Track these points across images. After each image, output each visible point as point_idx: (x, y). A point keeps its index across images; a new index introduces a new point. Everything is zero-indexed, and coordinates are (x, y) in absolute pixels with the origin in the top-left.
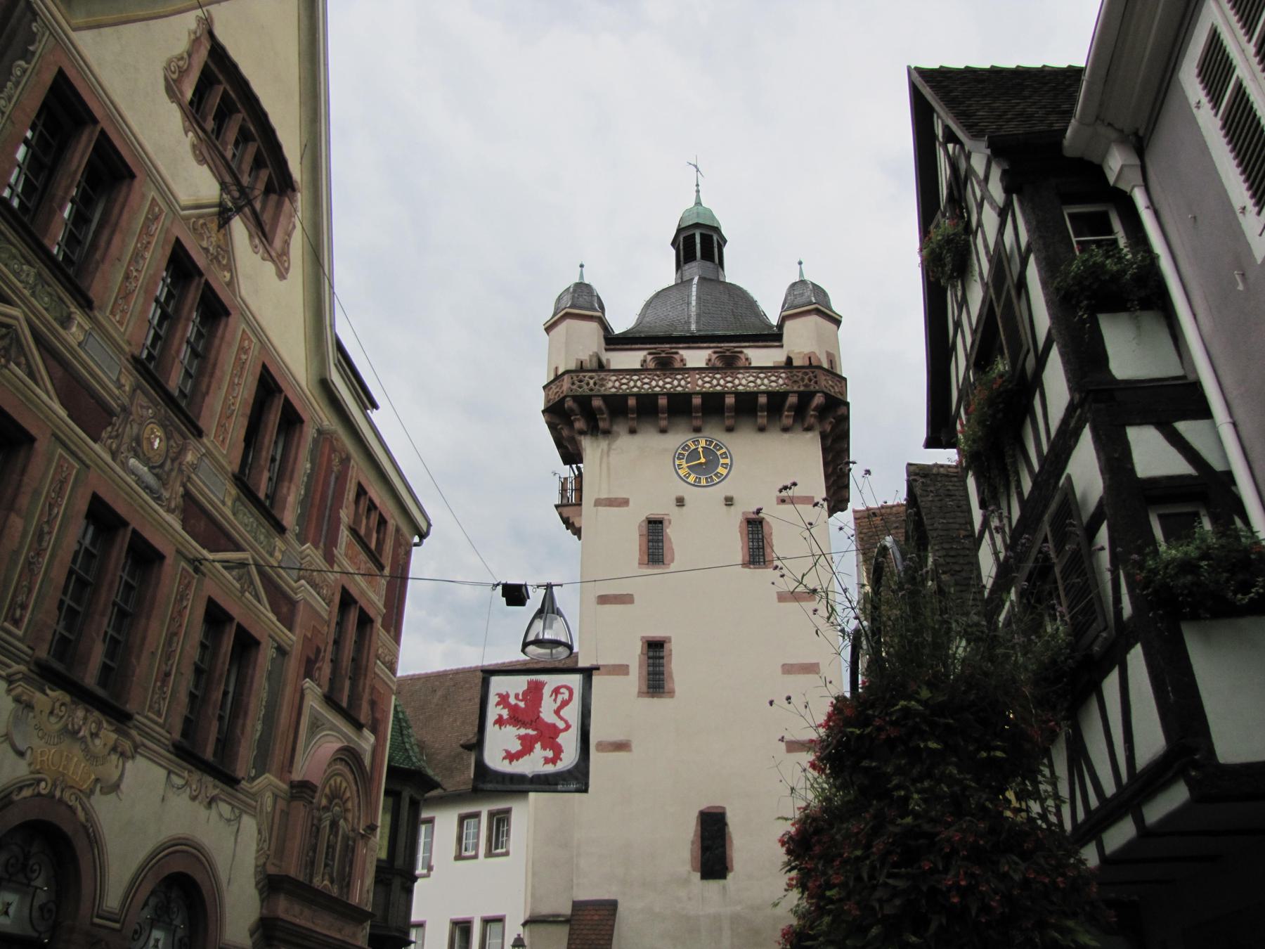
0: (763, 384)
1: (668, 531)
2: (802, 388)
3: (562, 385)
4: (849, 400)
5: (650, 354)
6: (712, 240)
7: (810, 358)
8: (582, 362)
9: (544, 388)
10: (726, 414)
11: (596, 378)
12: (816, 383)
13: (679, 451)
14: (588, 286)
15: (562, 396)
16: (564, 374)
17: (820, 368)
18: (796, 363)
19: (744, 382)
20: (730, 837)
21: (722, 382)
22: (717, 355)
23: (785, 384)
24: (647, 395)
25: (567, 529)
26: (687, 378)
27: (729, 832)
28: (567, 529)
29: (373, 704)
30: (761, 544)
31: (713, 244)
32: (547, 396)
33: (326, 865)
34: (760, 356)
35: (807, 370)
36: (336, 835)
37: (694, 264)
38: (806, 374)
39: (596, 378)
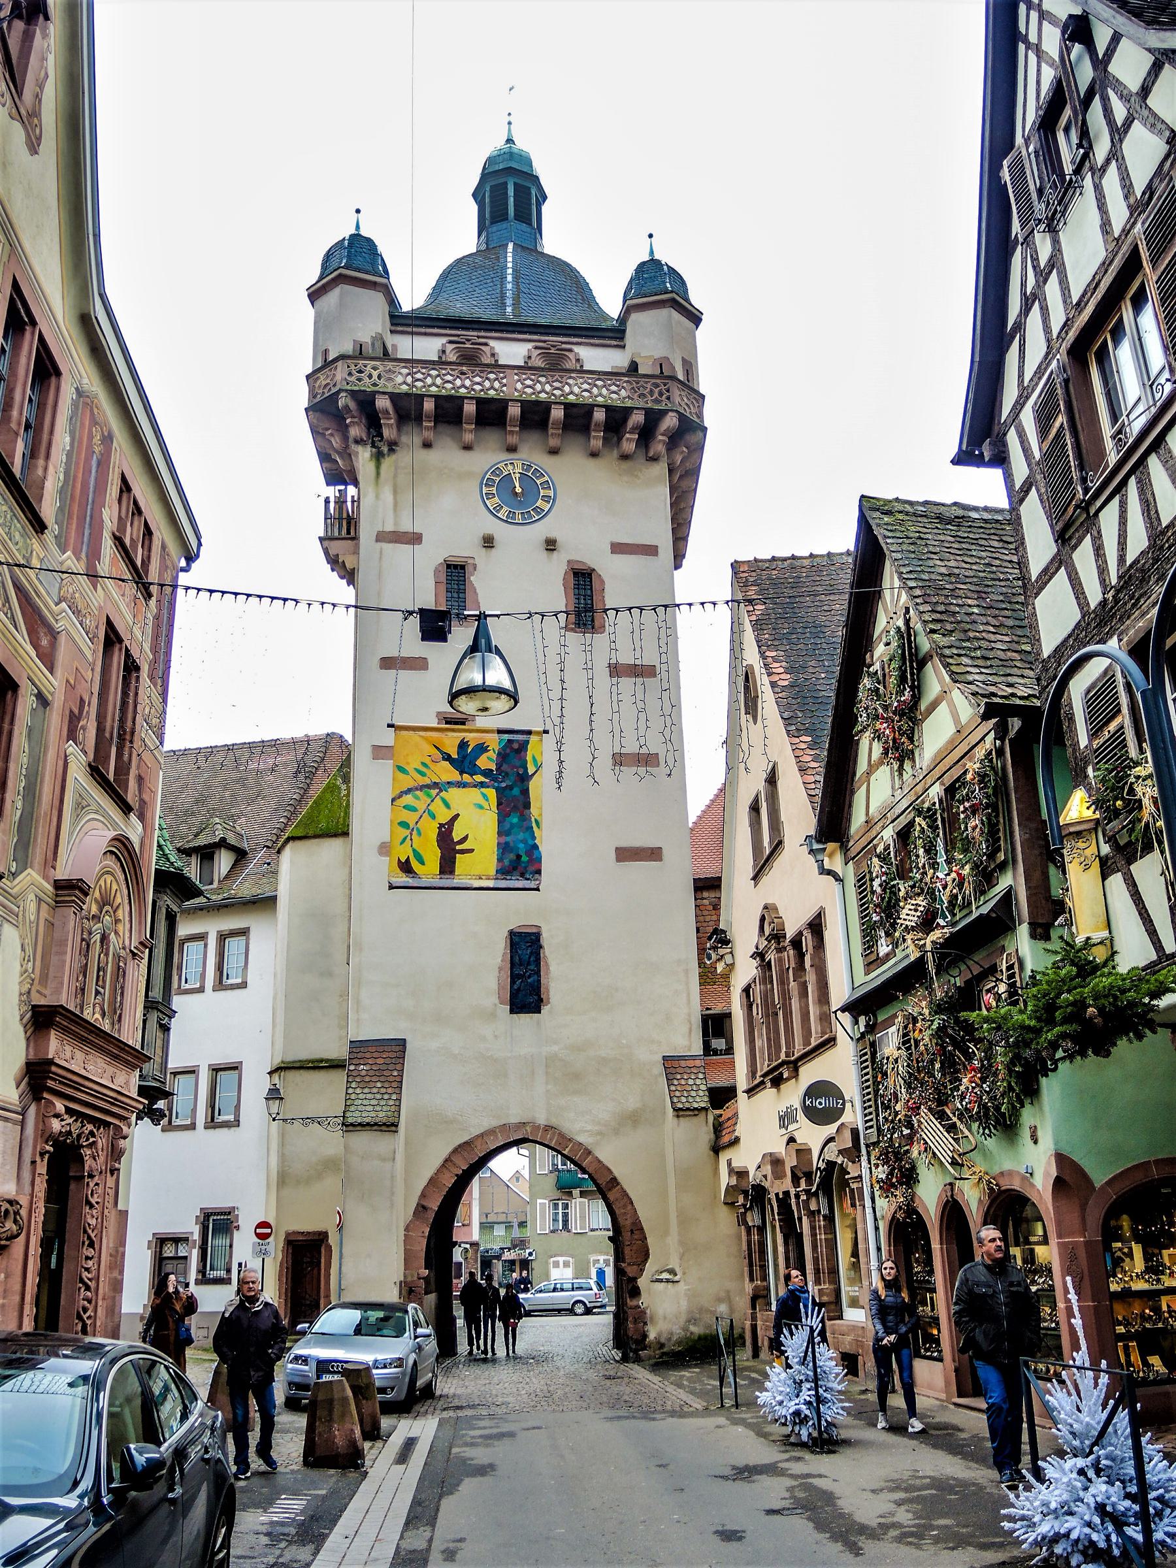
0: (600, 395)
1: (472, 578)
2: (649, 405)
4: (707, 423)
5: (451, 342)
6: (530, 193)
7: (661, 365)
9: (308, 377)
10: (551, 431)
11: (381, 368)
12: (668, 398)
13: (487, 476)
14: (369, 241)
15: (334, 390)
17: (673, 378)
18: (642, 370)
19: (576, 390)
20: (547, 964)
22: (540, 351)
23: (629, 397)
26: (502, 378)
27: (545, 956)
28: (333, 570)
29: (140, 779)
30: (589, 602)
31: (530, 199)
33: (97, 993)
34: (595, 357)
35: (658, 381)
36: (107, 955)
37: (504, 225)
38: (657, 386)
39: (381, 368)
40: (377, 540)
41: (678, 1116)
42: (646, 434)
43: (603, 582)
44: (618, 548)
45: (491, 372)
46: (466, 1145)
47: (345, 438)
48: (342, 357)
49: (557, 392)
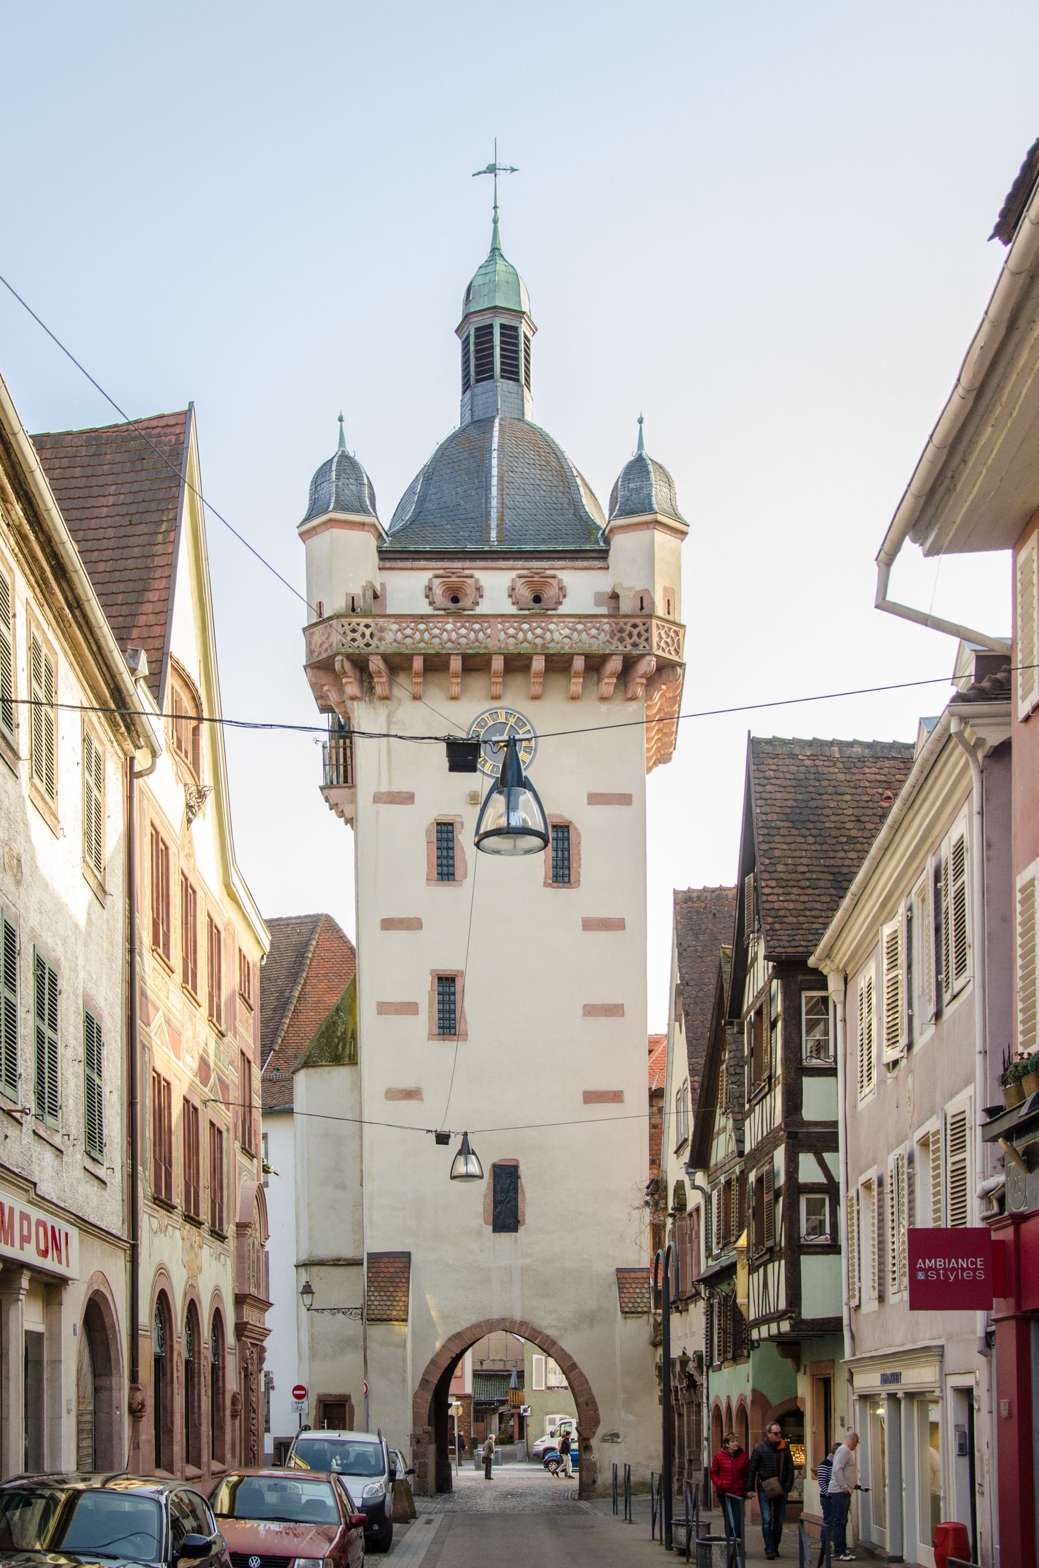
1: (460, 837)
3: (329, 635)
5: (437, 577)
6: (517, 337)
7: (642, 598)
8: (353, 598)
9: (305, 630)
12: (647, 640)
15: (330, 653)
16: (330, 618)
19: (556, 636)
20: (523, 1191)
21: (530, 636)
24: (438, 655)
25: (331, 809)
26: (486, 629)
28: (331, 809)
32: (309, 644)
35: (637, 621)
40: (374, 802)
41: (625, 1318)
42: (625, 674)
43: (579, 835)
44: (595, 799)
45: (476, 622)
46: (458, 1336)
47: (341, 689)
48: (338, 616)
49: (539, 641)
